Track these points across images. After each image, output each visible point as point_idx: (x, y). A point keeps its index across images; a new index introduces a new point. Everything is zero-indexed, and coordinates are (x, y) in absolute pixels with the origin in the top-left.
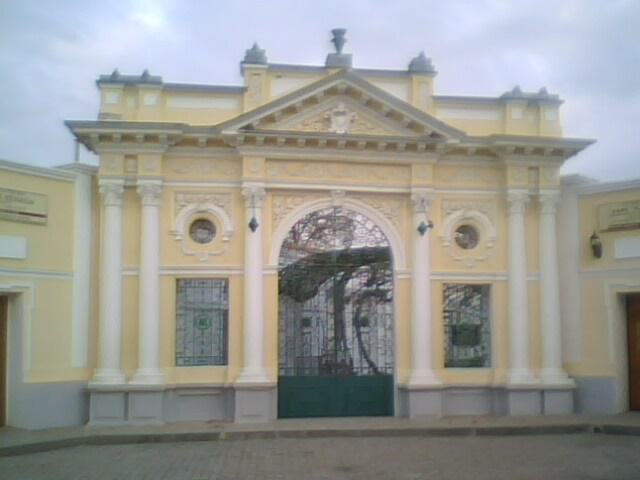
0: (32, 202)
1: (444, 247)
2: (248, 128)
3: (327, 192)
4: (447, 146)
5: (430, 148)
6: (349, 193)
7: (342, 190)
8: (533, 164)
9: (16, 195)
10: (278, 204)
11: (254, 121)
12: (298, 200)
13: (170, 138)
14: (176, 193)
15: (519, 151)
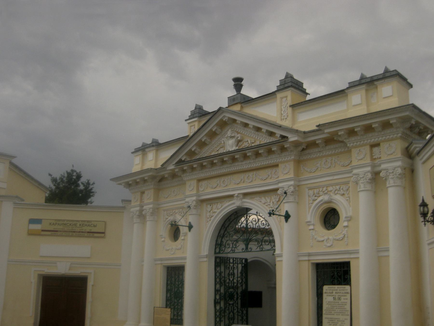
0: (95, 226)
1: (310, 230)
2: (180, 162)
3: (232, 196)
4: (296, 144)
5: (283, 149)
6: (245, 195)
7: (239, 194)
8: (373, 140)
9: (86, 223)
10: (209, 210)
11: (182, 156)
12: (219, 205)
13: (153, 178)
14: (164, 211)
15: (352, 132)
